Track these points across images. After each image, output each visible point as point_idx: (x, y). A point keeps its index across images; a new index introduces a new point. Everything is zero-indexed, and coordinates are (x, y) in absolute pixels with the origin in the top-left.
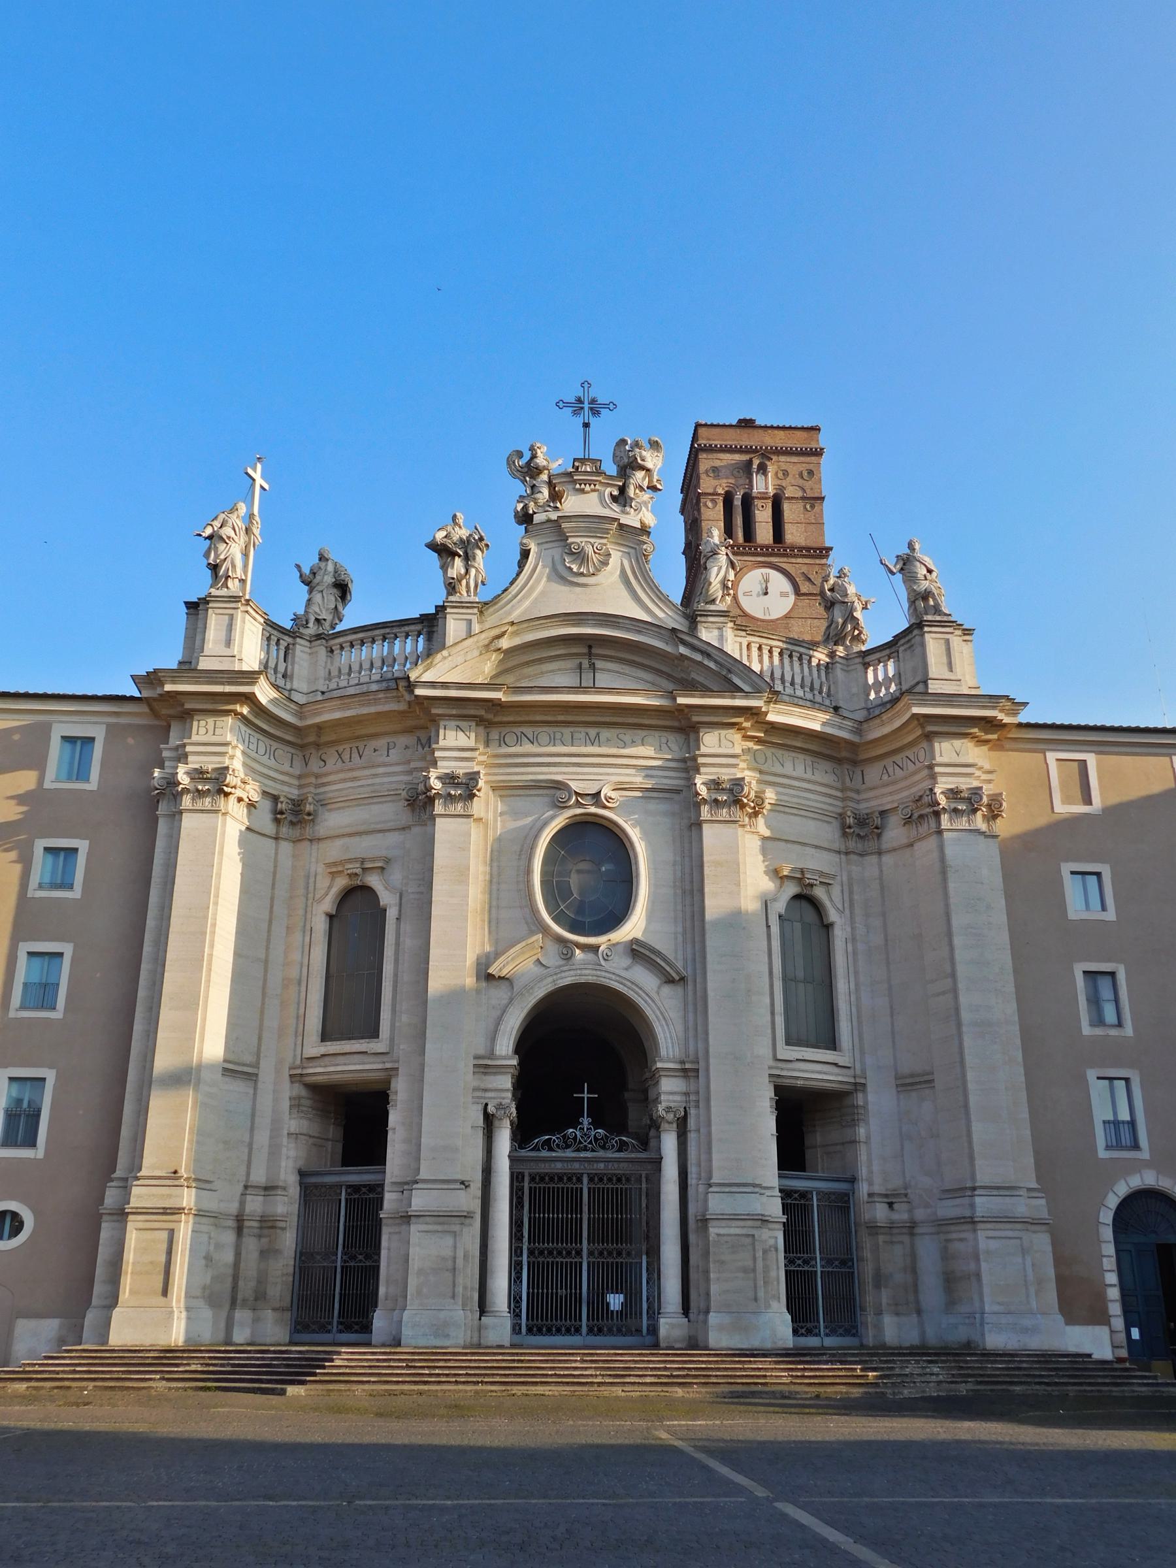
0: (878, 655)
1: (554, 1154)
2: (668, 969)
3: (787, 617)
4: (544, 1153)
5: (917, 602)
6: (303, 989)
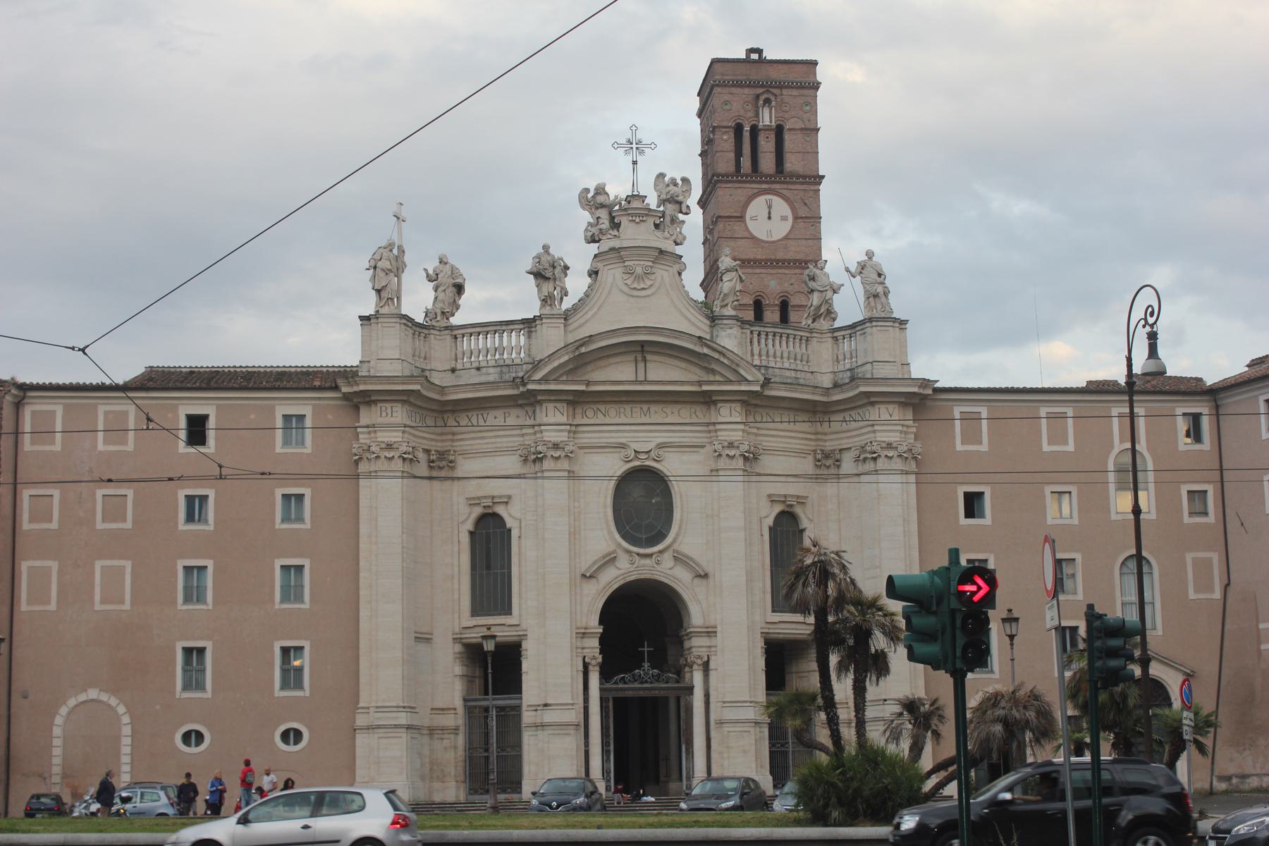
0: (843, 333)
1: (626, 686)
2: (697, 568)
3: (786, 238)
4: (621, 686)
5: (870, 299)
6: (456, 581)
